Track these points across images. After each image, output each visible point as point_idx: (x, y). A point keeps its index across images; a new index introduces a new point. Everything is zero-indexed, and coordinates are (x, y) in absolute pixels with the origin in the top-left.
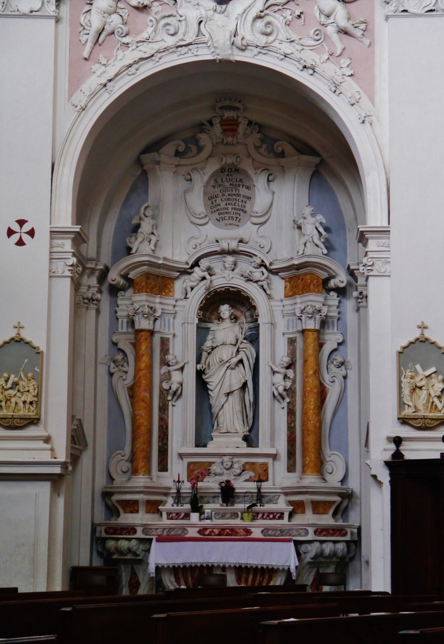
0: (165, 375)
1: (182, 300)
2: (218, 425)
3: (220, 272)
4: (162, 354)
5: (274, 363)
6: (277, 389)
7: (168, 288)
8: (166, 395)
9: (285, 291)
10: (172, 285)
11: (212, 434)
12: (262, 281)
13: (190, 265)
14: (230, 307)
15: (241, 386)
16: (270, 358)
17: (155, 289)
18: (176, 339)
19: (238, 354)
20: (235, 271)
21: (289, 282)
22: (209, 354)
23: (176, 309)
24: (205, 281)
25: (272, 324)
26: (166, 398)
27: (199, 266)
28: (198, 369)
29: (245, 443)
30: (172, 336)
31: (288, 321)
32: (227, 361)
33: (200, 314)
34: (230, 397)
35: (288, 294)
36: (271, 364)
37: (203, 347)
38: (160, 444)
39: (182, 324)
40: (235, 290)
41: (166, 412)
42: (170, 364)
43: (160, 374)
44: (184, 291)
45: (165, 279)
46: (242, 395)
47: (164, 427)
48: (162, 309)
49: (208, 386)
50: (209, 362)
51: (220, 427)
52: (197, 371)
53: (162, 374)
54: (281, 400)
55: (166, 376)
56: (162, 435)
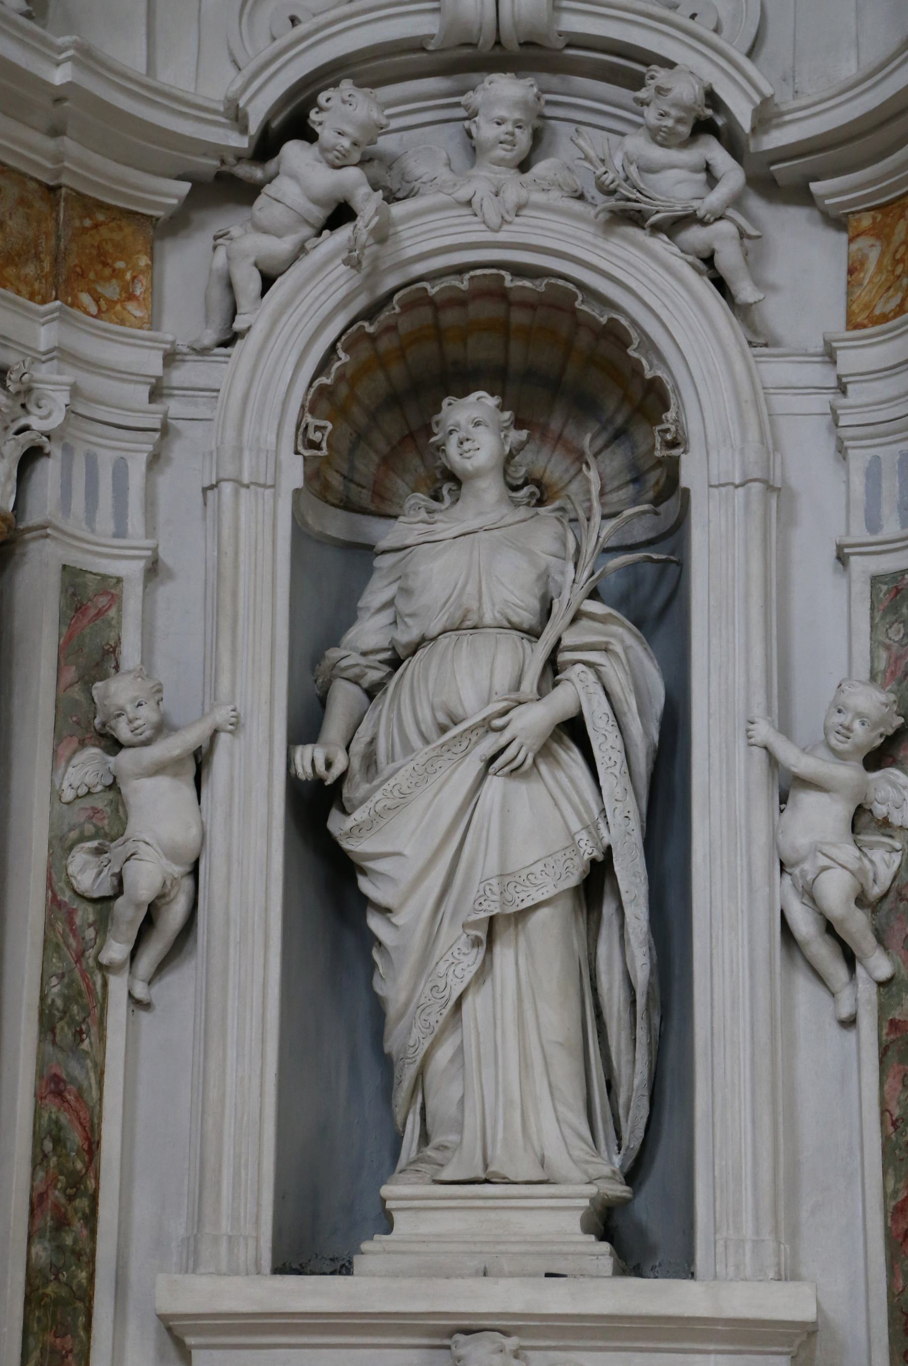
0: (88, 803)
1: (203, 352)
2: (425, 1138)
3: (444, 174)
4: (71, 674)
5: (785, 728)
6: (810, 895)
7: (116, 274)
8: (90, 933)
9: (849, 293)
10: (143, 261)
11: (386, 1190)
12: (703, 223)
13: (254, 127)
14: (502, 408)
15: (573, 880)
16: (759, 698)
17: (30, 270)
18: (164, 592)
19: (556, 684)
20: (540, 168)
21: (880, 233)
22: (372, 692)
23: (175, 407)
24: (345, 233)
25: (770, 488)
26: (91, 952)
27: (311, 137)
28: (303, 770)
29: (605, 1247)
30: (141, 565)
31: (873, 474)
32: (487, 727)
33: (316, 436)
34: (504, 955)
35: (867, 306)
36: (764, 731)
37: (333, 654)
38: (42, 1252)
39: (205, 490)
40: (541, 286)
41: (85, 1045)
42: (123, 732)
43: (56, 795)
44: (218, 294)
45: (101, 217)
46: (578, 945)
47: (75, 1138)
48: (75, 391)
49: (365, 885)
50: (373, 741)
51: (442, 1148)
52: (293, 782)
53: (68, 795)
54: (837, 970)
55: (95, 811)
56: (56, 1195)
